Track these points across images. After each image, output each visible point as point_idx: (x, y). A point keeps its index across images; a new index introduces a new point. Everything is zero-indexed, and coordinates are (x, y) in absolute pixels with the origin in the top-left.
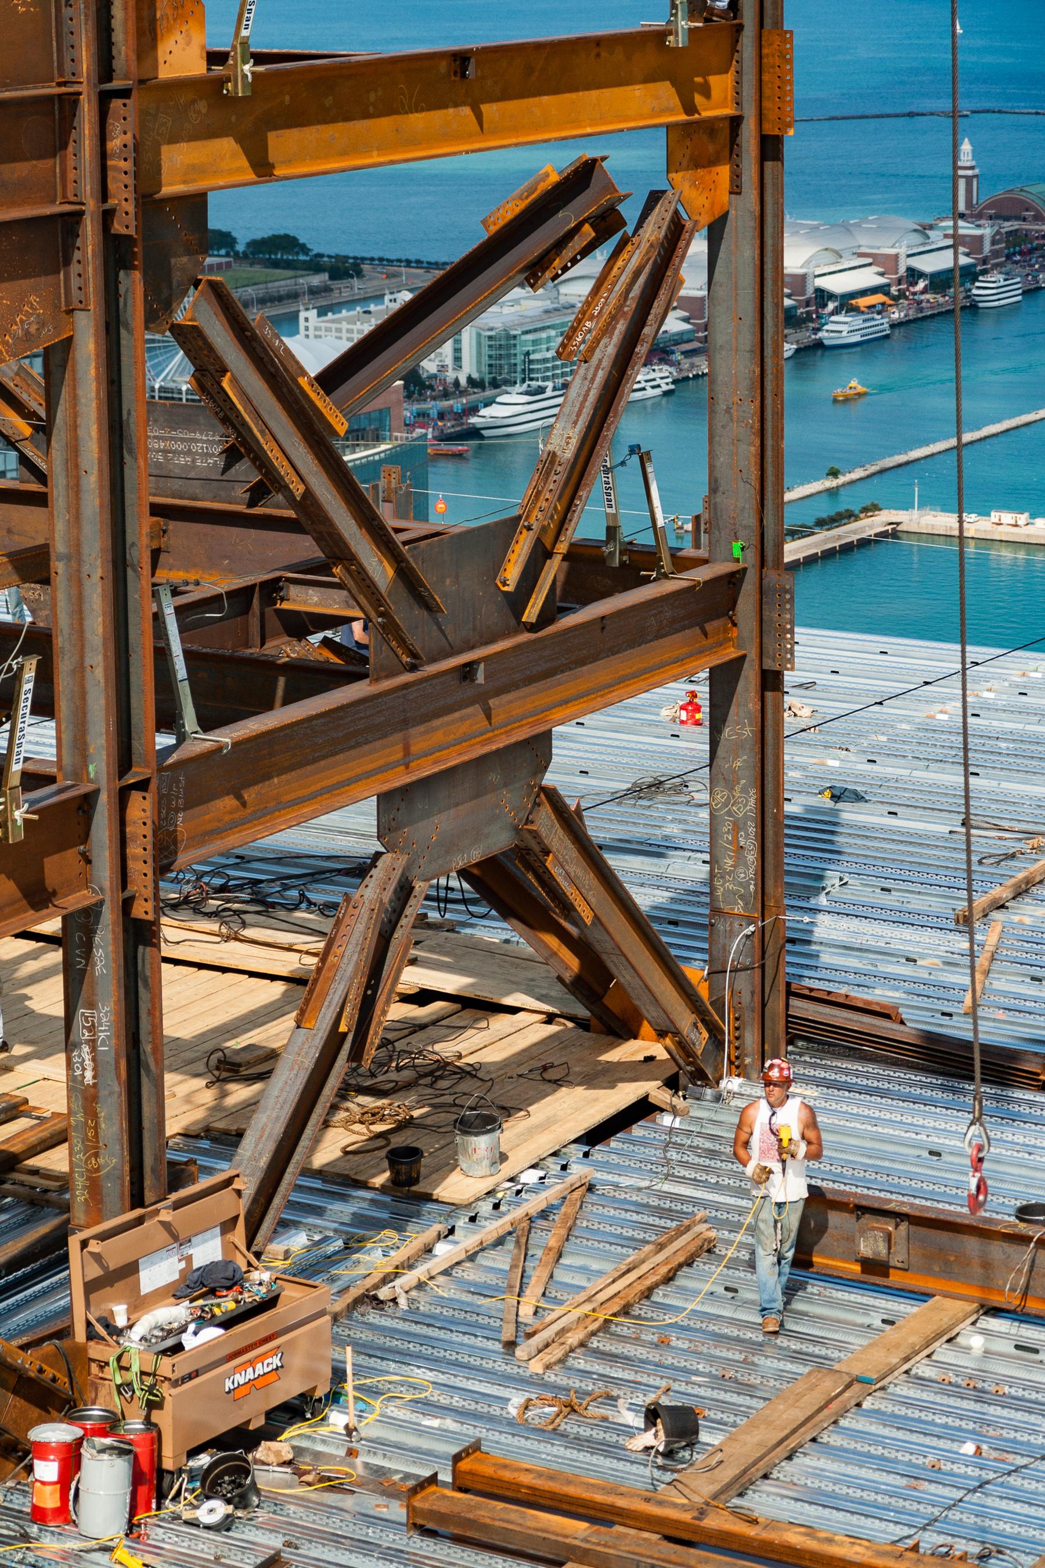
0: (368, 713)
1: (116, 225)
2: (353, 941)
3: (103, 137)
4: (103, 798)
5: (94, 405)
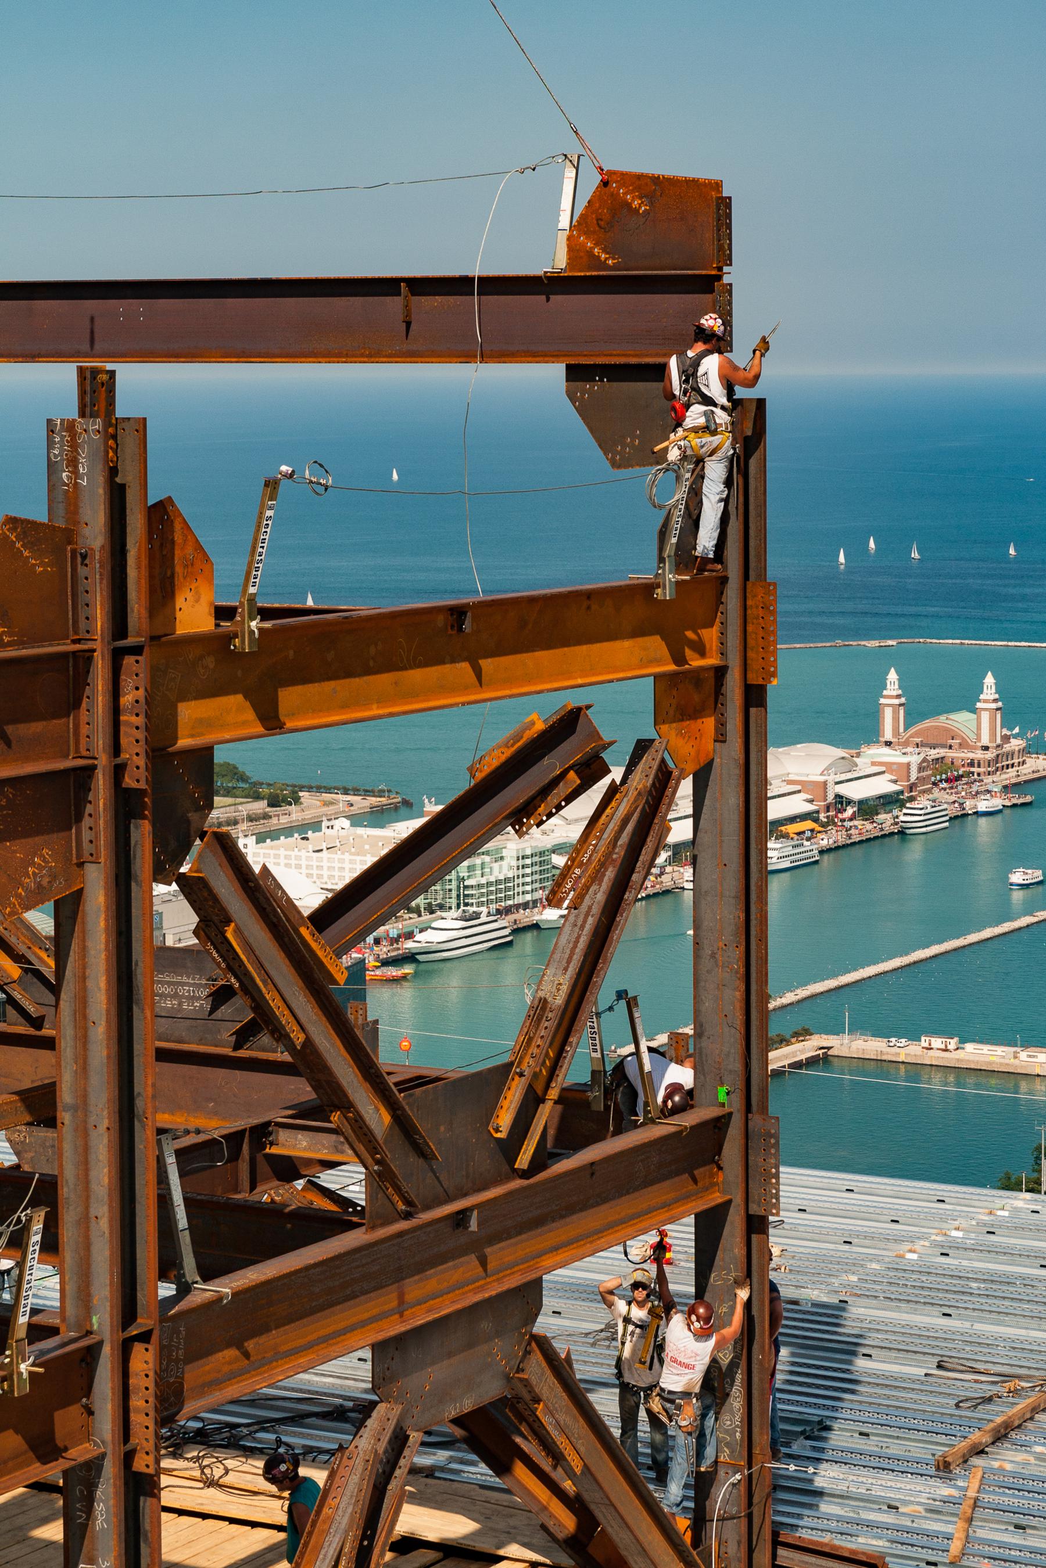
0: (364, 1261)
1: (127, 779)
2: (348, 1493)
3: (116, 693)
4: (106, 1350)
5: (103, 956)
